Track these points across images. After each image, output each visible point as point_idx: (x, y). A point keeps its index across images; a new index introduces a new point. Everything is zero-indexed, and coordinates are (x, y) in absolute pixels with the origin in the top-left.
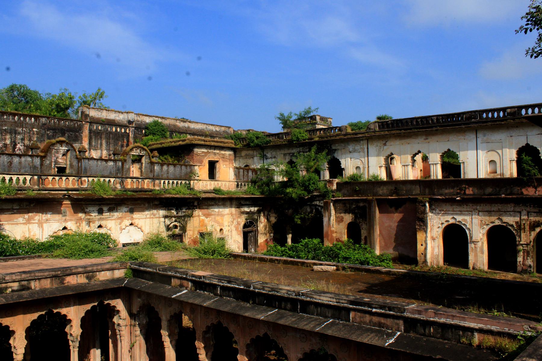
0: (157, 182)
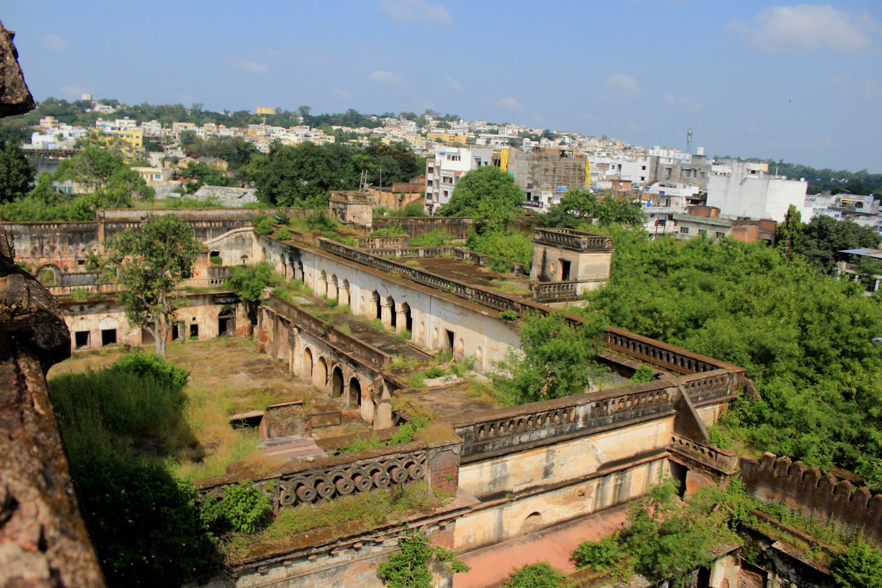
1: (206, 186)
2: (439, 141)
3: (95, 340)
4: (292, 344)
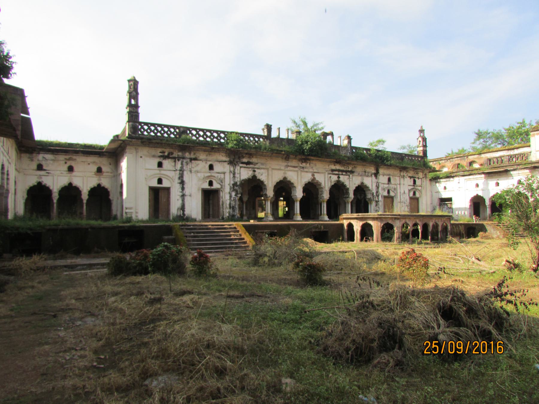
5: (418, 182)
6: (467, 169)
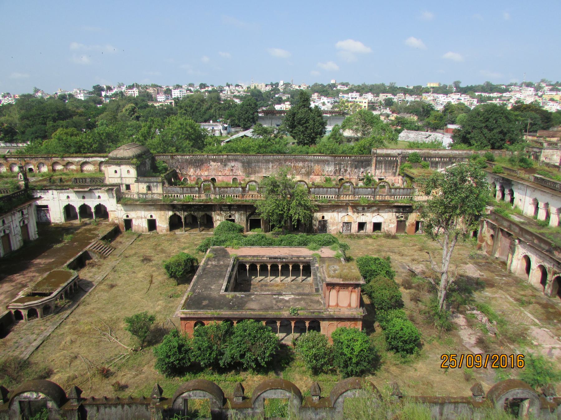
0: (393, 197)
1: (405, 130)
2: (552, 100)
3: (369, 228)
4: (512, 250)
5: (25, 212)
6: (59, 184)
